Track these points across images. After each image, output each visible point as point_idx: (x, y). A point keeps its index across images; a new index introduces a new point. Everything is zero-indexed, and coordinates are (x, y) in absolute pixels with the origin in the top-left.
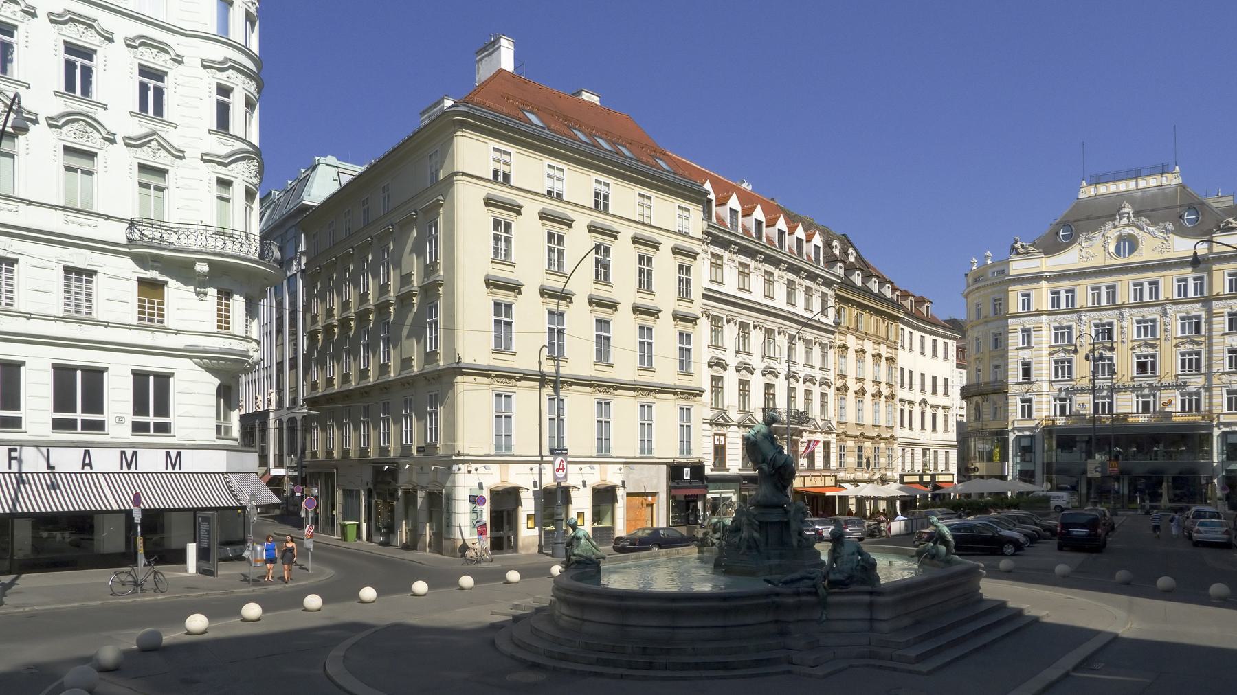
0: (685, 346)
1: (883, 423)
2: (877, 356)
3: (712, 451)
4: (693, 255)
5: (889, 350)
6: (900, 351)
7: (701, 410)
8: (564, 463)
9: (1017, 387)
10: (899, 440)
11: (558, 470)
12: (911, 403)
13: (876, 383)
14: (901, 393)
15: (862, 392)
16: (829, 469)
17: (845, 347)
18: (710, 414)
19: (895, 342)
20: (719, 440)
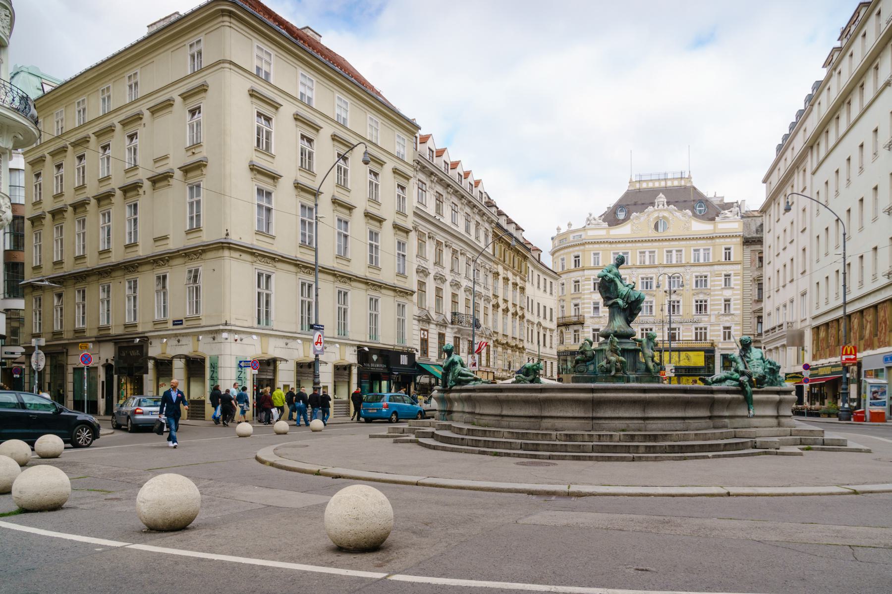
0: (401, 252)
1: (517, 336)
2: (515, 284)
3: (419, 343)
4: (407, 178)
5: (522, 282)
6: (527, 283)
7: (412, 309)
9: (591, 320)
10: (527, 350)
11: (317, 343)
12: (533, 323)
13: (515, 305)
14: (528, 316)
15: (506, 311)
16: (489, 366)
17: (497, 274)
18: (416, 311)
19: (525, 276)
20: (423, 334)
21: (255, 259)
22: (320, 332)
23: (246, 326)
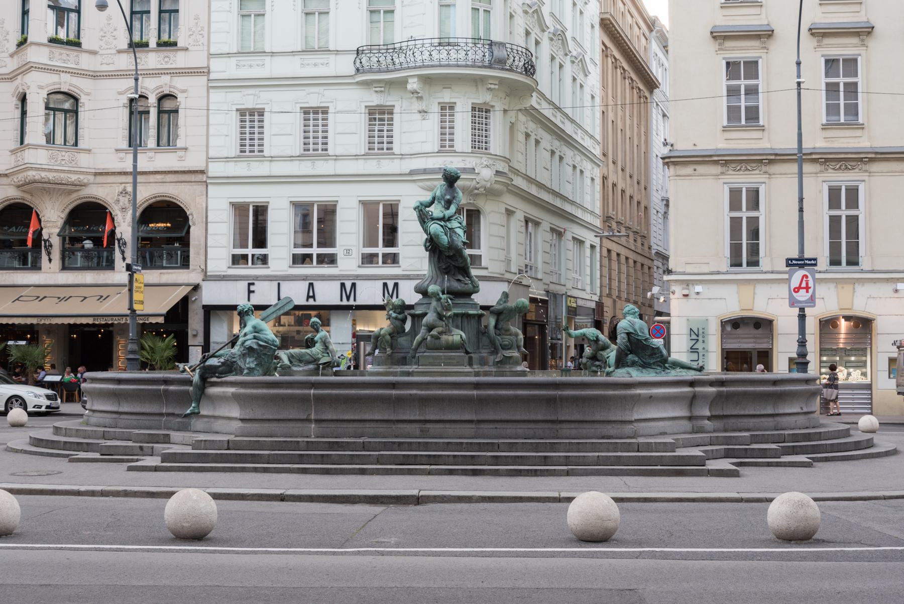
8: (810, 278)
11: (797, 290)
21: (724, 169)
22: (807, 270)
23: (707, 271)
